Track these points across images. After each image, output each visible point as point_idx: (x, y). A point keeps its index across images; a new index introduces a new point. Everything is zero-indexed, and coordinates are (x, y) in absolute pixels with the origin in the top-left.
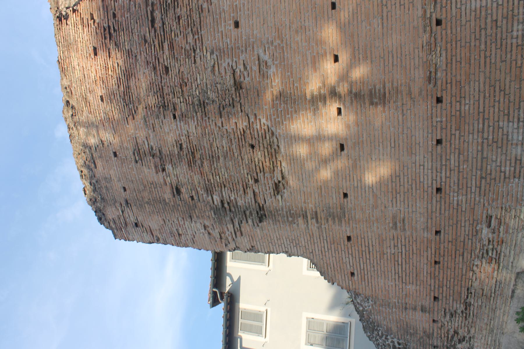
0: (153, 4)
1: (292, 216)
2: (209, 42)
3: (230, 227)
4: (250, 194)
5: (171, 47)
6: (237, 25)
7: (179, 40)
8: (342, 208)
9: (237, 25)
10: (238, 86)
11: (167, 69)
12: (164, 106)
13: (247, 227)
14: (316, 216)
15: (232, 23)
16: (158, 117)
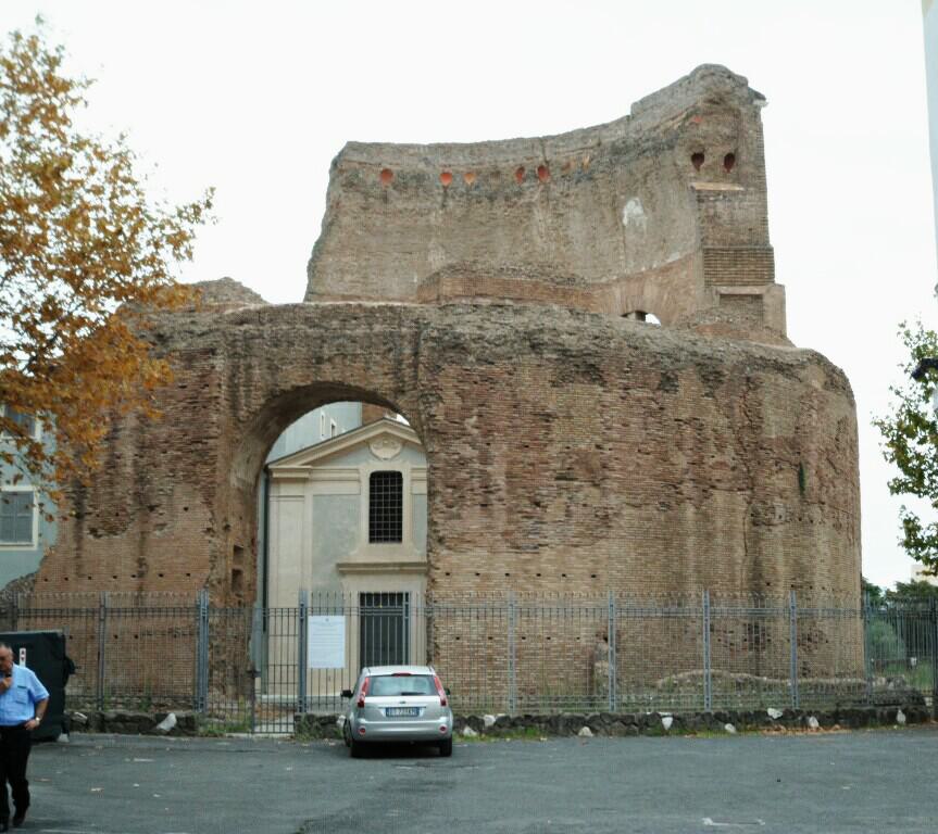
0: (206, 443)
1: (79, 539)
2: (179, 489)
3: (70, 490)
4: (90, 509)
5: (178, 458)
6: (186, 509)
7: (181, 465)
8: (83, 576)
9: (186, 509)
10: (152, 508)
11: (165, 452)
12: (142, 447)
13: (71, 502)
14: (78, 557)
15: (187, 506)
16: (137, 441)
